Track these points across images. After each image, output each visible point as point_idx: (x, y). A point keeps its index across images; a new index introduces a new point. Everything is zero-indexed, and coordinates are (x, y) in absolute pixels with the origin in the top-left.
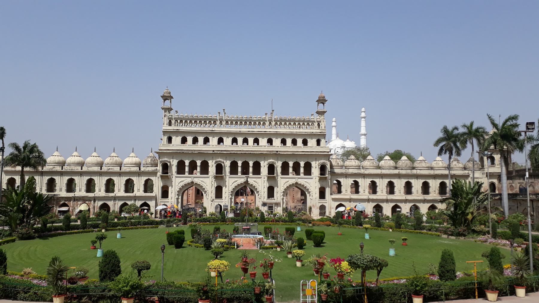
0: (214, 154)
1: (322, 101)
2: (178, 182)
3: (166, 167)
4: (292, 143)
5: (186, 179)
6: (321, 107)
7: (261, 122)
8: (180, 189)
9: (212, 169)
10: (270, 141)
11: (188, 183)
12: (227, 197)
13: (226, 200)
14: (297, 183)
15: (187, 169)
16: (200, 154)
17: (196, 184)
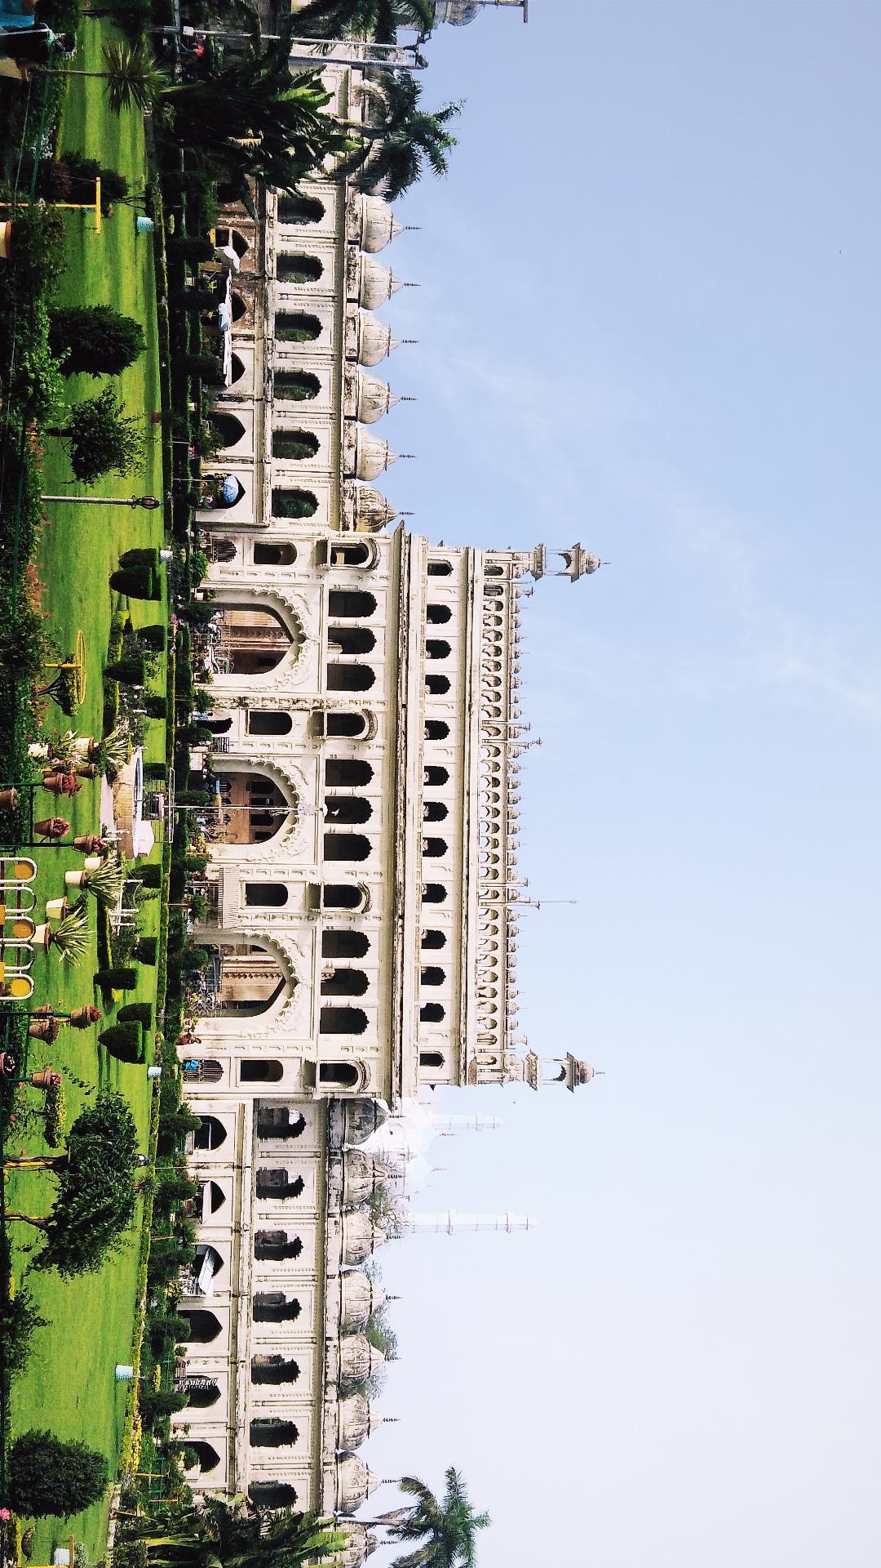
0: (398, 708)
1: (575, 1075)
2: (304, 590)
3: (355, 555)
4: (429, 969)
5: (316, 620)
6: (549, 1070)
7: (502, 864)
8: (283, 601)
9: (347, 702)
10: (435, 893)
11: (299, 627)
12: (249, 750)
13: (244, 746)
14: (295, 982)
15: (348, 622)
16: (398, 664)
17: (299, 650)
